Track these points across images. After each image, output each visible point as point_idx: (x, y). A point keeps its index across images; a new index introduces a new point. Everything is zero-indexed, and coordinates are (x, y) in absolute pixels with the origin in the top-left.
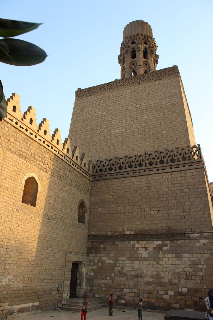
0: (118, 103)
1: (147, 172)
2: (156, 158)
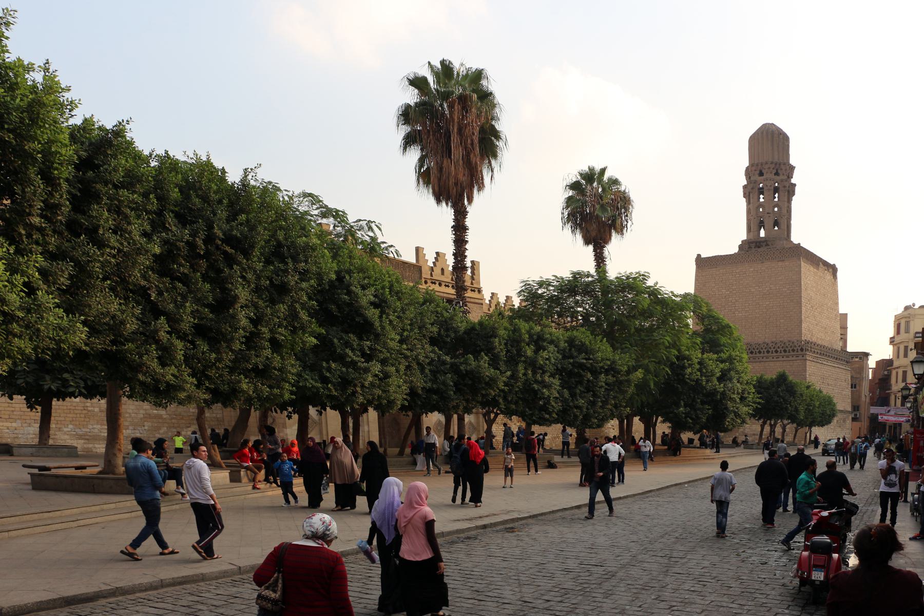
0: (741, 282)
1: (765, 359)
2: (772, 347)
